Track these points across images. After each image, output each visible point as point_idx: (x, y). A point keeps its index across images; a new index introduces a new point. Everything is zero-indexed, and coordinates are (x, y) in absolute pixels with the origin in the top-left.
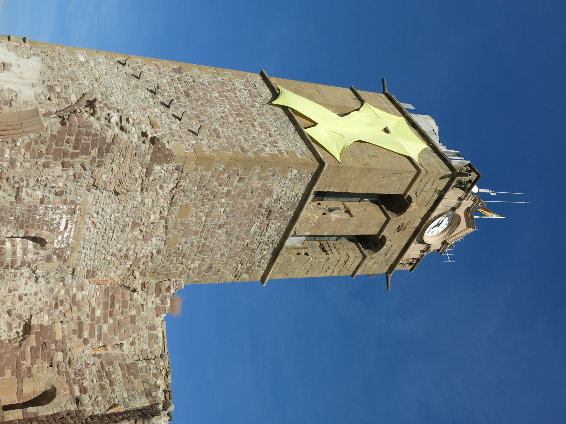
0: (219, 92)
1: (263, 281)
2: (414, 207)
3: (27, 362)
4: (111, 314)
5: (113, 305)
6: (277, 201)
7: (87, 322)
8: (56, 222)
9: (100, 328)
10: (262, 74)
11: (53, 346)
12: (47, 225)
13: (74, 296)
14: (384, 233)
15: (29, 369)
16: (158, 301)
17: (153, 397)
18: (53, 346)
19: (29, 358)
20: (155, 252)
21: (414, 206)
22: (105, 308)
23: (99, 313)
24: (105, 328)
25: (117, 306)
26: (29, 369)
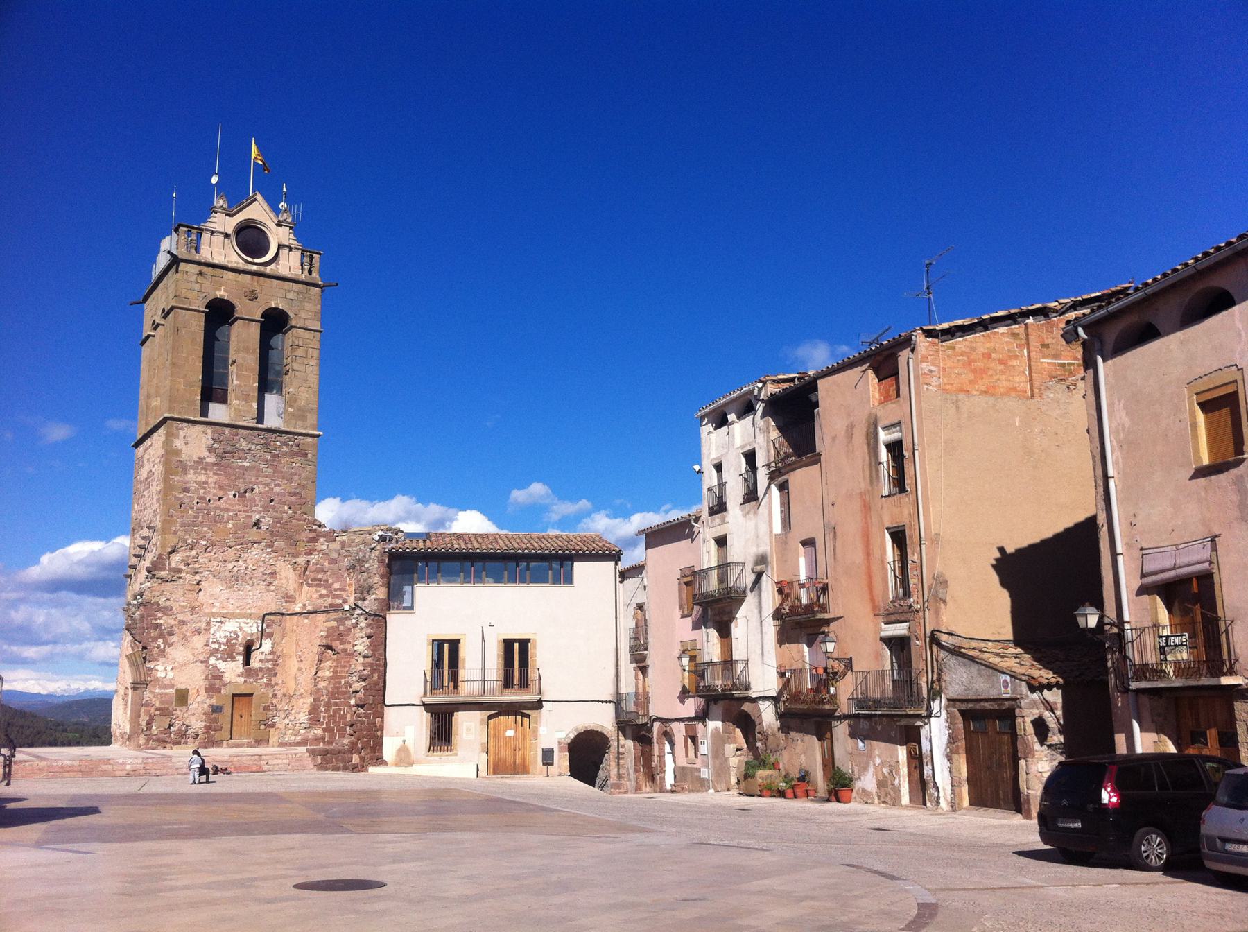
1: (318, 436)
4: (326, 581)
5: (320, 580)
6: (210, 449)
10: (137, 445)
11: (341, 628)
14: (258, 316)
21: (221, 293)
22: (319, 586)
23: (324, 592)
24: (337, 586)
25: (320, 576)
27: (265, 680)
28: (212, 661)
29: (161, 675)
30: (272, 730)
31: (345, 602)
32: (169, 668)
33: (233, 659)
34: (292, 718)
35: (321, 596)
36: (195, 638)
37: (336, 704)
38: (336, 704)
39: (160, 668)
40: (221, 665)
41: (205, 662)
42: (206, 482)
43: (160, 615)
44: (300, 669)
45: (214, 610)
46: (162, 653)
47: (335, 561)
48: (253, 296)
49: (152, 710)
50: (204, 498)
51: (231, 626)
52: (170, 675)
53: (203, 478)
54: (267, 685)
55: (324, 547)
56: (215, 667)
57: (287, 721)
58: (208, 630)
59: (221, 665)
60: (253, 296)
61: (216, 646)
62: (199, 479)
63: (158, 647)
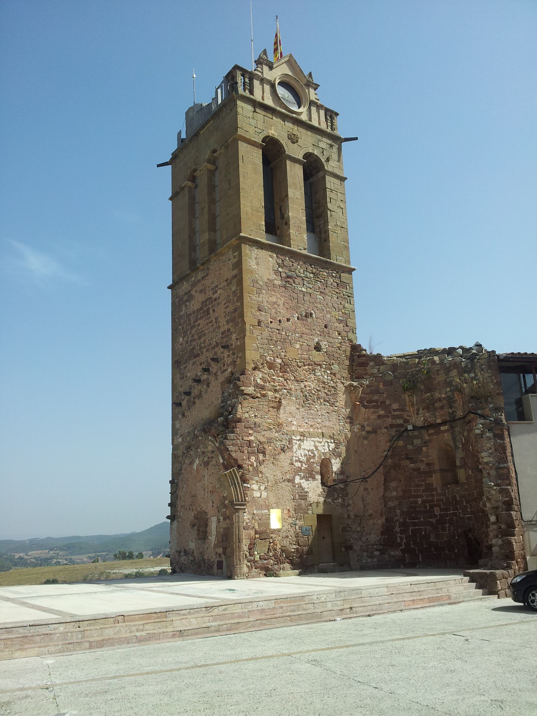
0: (192, 328)
2: (273, 132)
3: (423, 467)
4: (384, 402)
5: (376, 401)
6: (276, 272)
7: (389, 421)
8: (307, 452)
9: (395, 410)
12: (310, 458)
13: (368, 432)
14: (300, 157)
15: (428, 464)
16: (372, 364)
17: (450, 366)
18: (410, 447)
19: (419, 465)
20: (329, 372)
21: (272, 132)
22: (376, 407)
23: (382, 412)
24: (395, 406)
25: (376, 397)
26: (428, 464)
27: (340, 500)
28: (297, 480)
29: (257, 494)
30: (351, 552)
31: (406, 421)
32: (262, 488)
33: (314, 479)
34: (364, 539)
35: (379, 417)
36: (282, 456)
37: (415, 524)
38: (415, 524)
39: (255, 487)
40: (305, 484)
41: (291, 481)
42: (275, 303)
43: (251, 432)
44: (366, 489)
45: (293, 428)
46: (257, 471)
47: (388, 383)
48: (293, 139)
49: (252, 533)
50: (275, 319)
51: (308, 444)
52: (264, 494)
53: (274, 300)
54: (342, 505)
55: (375, 371)
56: (300, 486)
57: (360, 543)
58: (290, 449)
59: (305, 484)
60: (293, 139)
61: (299, 464)
62: (271, 299)
63: (252, 465)
